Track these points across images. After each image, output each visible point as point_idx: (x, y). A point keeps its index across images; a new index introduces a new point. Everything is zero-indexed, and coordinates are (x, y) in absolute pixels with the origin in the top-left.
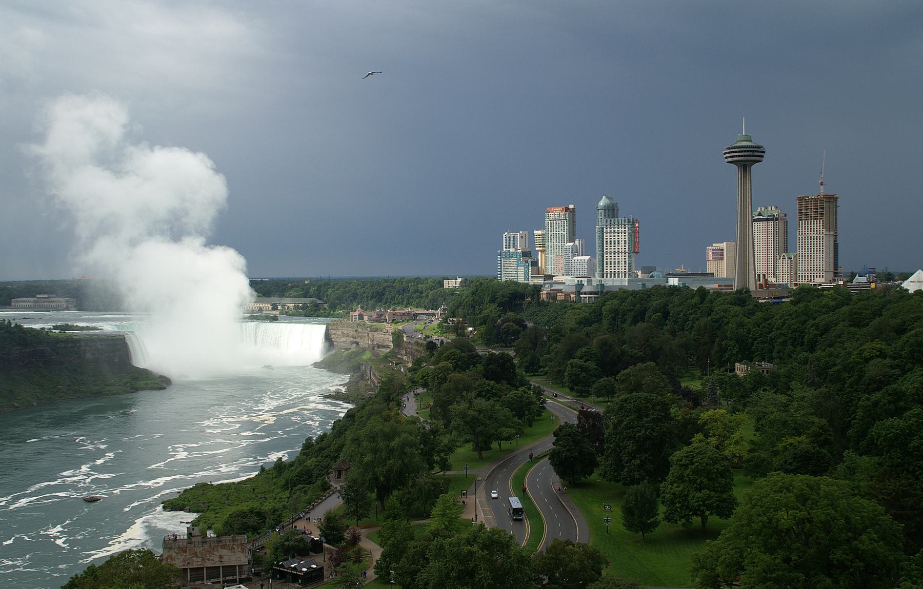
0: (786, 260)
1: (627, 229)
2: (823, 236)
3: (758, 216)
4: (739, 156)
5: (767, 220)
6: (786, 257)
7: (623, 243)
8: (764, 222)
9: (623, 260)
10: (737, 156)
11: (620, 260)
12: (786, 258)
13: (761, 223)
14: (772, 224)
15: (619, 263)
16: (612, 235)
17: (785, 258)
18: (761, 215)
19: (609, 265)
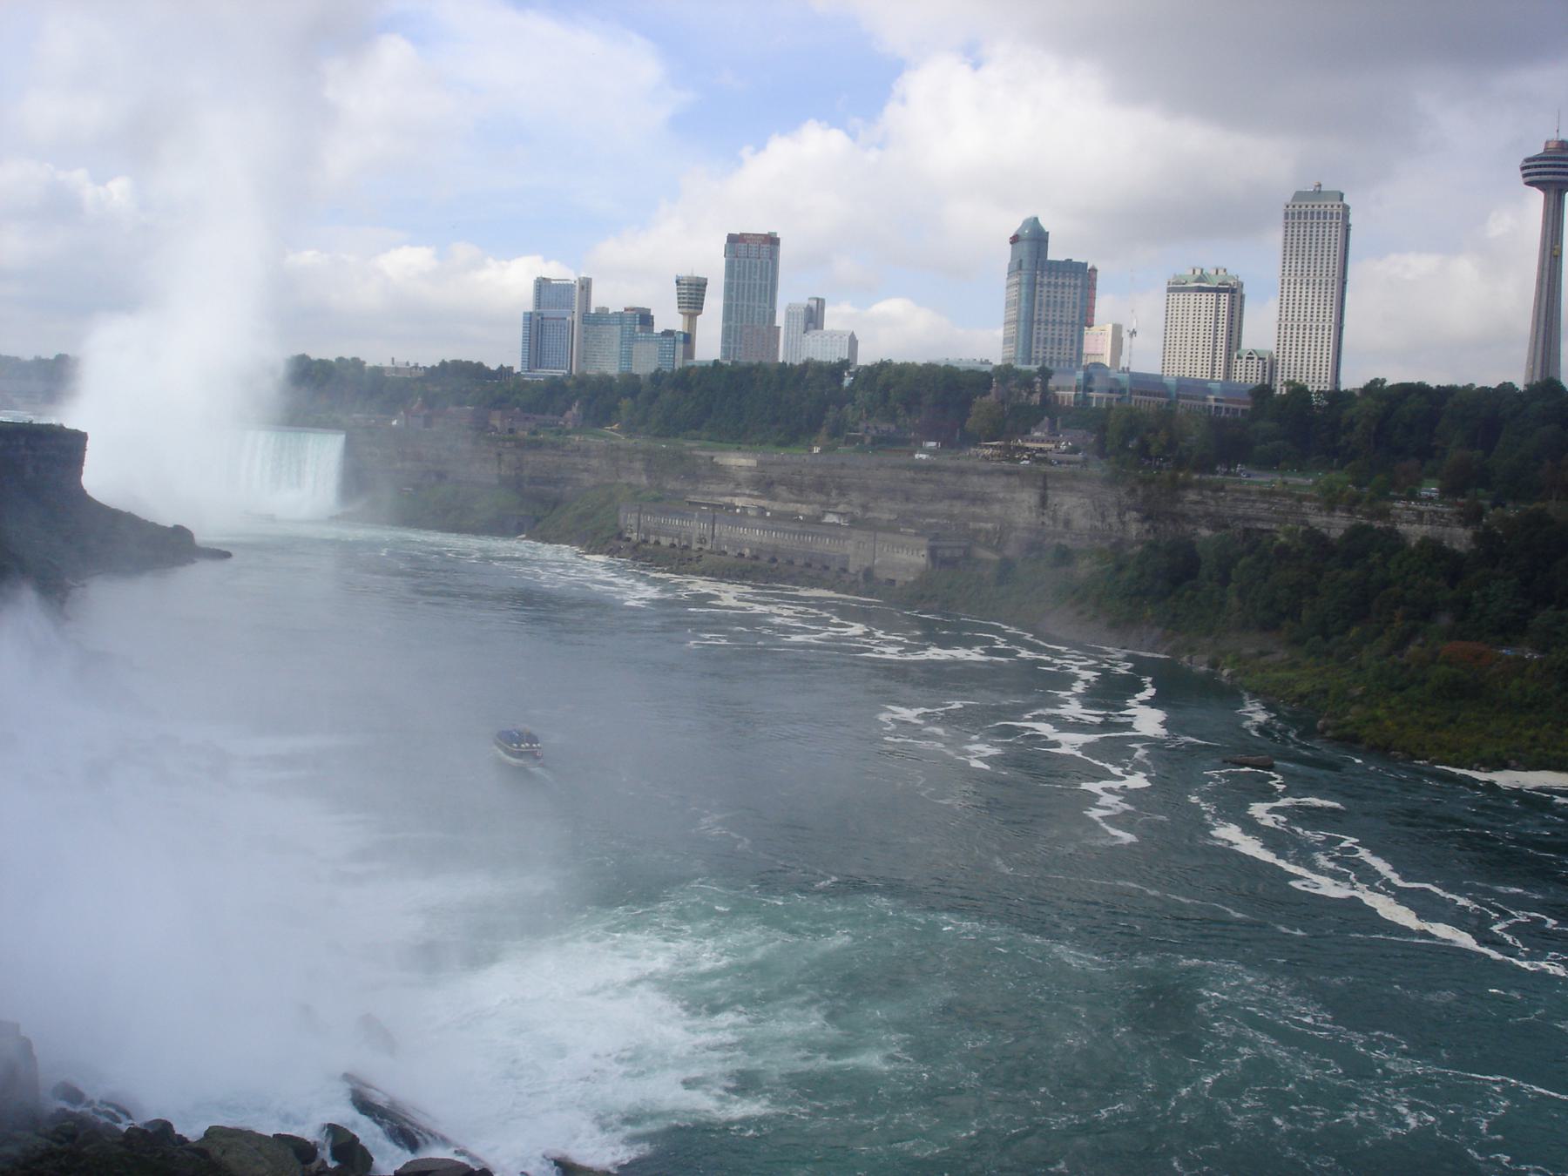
0: (1255, 360)
1: (1079, 282)
2: (1330, 326)
3: (1196, 282)
4: (1554, 173)
5: (1217, 290)
6: (1255, 356)
7: (1071, 307)
8: (1210, 294)
9: (1069, 338)
10: (1550, 173)
11: (1063, 337)
12: (1256, 358)
13: (1204, 295)
14: (1227, 298)
15: (1060, 344)
16: (1052, 289)
17: (1252, 358)
18: (1204, 282)
19: (1041, 345)
